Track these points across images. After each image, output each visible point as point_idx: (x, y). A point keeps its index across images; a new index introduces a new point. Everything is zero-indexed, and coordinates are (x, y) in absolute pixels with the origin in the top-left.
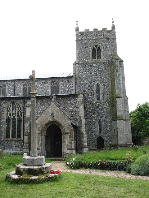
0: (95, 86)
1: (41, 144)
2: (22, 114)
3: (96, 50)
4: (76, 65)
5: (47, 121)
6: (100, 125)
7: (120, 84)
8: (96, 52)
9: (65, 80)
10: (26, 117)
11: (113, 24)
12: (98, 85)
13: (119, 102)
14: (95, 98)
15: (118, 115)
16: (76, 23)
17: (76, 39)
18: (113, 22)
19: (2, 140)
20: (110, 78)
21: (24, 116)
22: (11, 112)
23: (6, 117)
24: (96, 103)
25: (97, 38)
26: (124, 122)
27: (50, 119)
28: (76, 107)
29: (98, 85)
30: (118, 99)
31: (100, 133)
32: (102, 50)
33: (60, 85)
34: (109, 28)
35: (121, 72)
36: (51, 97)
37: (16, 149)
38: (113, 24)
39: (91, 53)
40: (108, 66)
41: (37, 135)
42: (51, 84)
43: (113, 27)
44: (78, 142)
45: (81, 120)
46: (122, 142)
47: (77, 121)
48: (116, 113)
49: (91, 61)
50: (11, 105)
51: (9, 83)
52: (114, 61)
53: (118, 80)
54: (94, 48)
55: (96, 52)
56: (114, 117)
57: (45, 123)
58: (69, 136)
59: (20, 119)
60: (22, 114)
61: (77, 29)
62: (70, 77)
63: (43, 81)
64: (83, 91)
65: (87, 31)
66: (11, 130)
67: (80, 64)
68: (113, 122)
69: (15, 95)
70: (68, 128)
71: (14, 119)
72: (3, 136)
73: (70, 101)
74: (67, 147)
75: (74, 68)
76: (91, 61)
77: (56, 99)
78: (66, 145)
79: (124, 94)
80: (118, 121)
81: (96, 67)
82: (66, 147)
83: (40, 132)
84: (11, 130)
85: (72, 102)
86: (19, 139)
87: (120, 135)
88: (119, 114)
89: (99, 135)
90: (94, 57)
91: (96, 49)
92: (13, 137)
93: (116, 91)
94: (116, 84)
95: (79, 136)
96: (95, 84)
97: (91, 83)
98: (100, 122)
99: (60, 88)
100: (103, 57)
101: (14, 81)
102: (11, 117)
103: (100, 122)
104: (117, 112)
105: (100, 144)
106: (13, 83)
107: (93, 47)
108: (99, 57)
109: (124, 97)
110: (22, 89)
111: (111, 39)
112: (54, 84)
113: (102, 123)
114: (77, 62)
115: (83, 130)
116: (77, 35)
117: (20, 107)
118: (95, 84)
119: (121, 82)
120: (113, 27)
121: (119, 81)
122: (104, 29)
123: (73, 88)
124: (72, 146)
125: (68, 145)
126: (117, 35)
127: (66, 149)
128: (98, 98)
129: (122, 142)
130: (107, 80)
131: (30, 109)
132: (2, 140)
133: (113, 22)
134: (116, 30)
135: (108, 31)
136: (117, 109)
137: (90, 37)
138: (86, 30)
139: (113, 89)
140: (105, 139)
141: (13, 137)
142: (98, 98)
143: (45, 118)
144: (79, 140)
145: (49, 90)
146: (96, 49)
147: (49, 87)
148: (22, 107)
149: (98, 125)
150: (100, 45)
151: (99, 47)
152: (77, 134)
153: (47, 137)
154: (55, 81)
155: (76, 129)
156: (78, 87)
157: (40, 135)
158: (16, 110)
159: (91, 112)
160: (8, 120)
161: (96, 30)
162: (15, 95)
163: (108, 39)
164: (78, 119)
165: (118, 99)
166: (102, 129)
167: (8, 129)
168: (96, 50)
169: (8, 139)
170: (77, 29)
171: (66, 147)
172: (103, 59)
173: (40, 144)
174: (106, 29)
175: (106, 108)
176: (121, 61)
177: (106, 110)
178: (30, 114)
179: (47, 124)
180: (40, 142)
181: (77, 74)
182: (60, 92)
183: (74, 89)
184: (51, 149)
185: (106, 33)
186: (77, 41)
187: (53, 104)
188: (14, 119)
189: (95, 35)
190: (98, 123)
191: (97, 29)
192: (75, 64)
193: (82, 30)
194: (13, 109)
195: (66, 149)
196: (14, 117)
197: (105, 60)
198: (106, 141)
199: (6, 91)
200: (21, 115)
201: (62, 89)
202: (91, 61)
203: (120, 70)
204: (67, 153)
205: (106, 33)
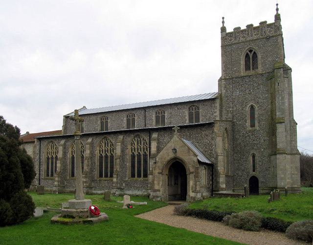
0: (248, 109)
1: (162, 185)
2: (148, 149)
3: (251, 57)
4: (222, 82)
5: (168, 158)
6: (254, 161)
7: (283, 103)
8: (251, 59)
9: (207, 103)
10: (152, 153)
11: (277, 13)
12: (252, 107)
13: (280, 129)
14: (248, 124)
15: (278, 147)
16: (275, 13)
17: (222, 44)
18: (277, 10)
19: (127, 179)
20: (270, 96)
21: (150, 152)
22: (136, 147)
23: (99, 155)
24: (250, 131)
25: (251, 38)
26: (289, 157)
27: (172, 155)
28: (213, 139)
29: (252, 107)
30: (279, 124)
31: (254, 171)
32: (259, 56)
33: (200, 110)
34: (271, 20)
35: (286, 86)
36: (173, 128)
37: (142, 190)
38: (223, 25)
39: (243, 62)
40: (267, 79)
41: (157, 174)
42: (190, 110)
43: (278, 17)
44: (215, 183)
45: (217, 156)
46: (282, 184)
47: (213, 157)
48: (276, 145)
49: (242, 74)
50: (136, 139)
51: (138, 112)
52: (275, 71)
53: (280, 98)
54: (247, 54)
55: (251, 59)
56: (274, 151)
57: (166, 160)
58: (195, 176)
59: (145, 155)
60: (148, 149)
61: (223, 29)
62: (212, 100)
63: (179, 107)
64: (231, 117)
65: (237, 30)
66: (136, 168)
67: (227, 80)
68: (273, 157)
69: (145, 125)
70: (193, 166)
71: (106, 156)
72: (127, 175)
73: (205, 132)
74: (192, 189)
75: (220, 86)
76: (243, 73)
77: (179, 131)
78: (191, 187)
79: (290, 117)
80: (278, 156)
81: (250, 81)
82: (190, 189)
83: (160, 171)
84: (136, 168)
85: (207, 132)
86: (145, 178)
87: (280, 175)
88: (280, 146)
89: (252, 173)
90: (247, 68)
91: (251, 55)
92: (139, 176)
93: (277, 114)
94: (277, 104)
95: (215, 176)
96: (248, 106)
97: (243, 104)
98: (254, 156)
99: (200, 114)
100: (260, 66)
101: (144, 109)
102: (136, 153)
103: (254, 156)
104: (278, 142)
105: (254, 187)
106: (143, 112)
107: (246, 54)
108: (255, 66)
109: (290, 121)
110: (154, 118)
111: (273, 37)
112: (193, 110)
113: (256, 158)
114: (223, 78)
115: (221, 168)
116: (223, 39)
117: (145, 140)
118: (248, 106)
119: (286, 101)
120: (278, 17)
121: (283, 98)
122: (263, 24)
123: (218, 113)
124: (196, 188)
125: (192, 187)
126: (284, 30)
127: (191, 191)
128: (253, 125)
129: (282, 184)
130: (266, 98)
131: (155, 143)
132: (127, 179)
133: (277, 10)
134: (283, 23)
135: (270, 25)
136: (277, 138)
137: (242, 39)
138: (235, 29)
139: (273, 112)
140: (261, 180)
141: (106, 176)
142: (253, 125)
143: (166, 155)
144: (215, 180)
145: (187, 118)
146: (251, 55)
147: (187, 113)
148: (148, 141)
149: (252, 161)
150: (255, 48)
151: (255, 53)
152: (213, 173)
153: (170, 176)
154: (194, 106)
155: (211, 168)
156: (224, 112)
157: (161, 175)
158: (141, 145)
159: (242, 144)
160: (133, 156)
161: (250, 27)
162: (145, 125)
163: (268, 38)
164: (215, 155)
165: (278, 126)
166: (257, 166)
167: (133, 166)
168: (251, 57)
169: (133, 179)
170: (223, 29)
171: (190, 189)
172: (260, 69)
173: (160, 185)
174: (266, 22)
175: (263, 138)
176: (287, 70)
177: (262, 141)
178: (156, 150)
179: (169, 161)
180: (161, 183)
181: (223, 95)
182: (201, 119)
183: (218, 115)
184: (181, 191)
185: (267, 30)
186: (223, 47)
187: (176, 137)
188: (139, 155)
189: (248, 34)
190: (251, 158)
191: (252, 25)
192: (220, 80)
193: (230, 29)
194: (138, 144)
195: (191, 191)
196: (139, 153)
197: (263, 70)
198: (262, 182)
199: (136, 121)
200: (147, 150)
201: (202, 116)
202: (243, 73)
203: (286, 82)
204: (192, 197)
205: (267, 30)
